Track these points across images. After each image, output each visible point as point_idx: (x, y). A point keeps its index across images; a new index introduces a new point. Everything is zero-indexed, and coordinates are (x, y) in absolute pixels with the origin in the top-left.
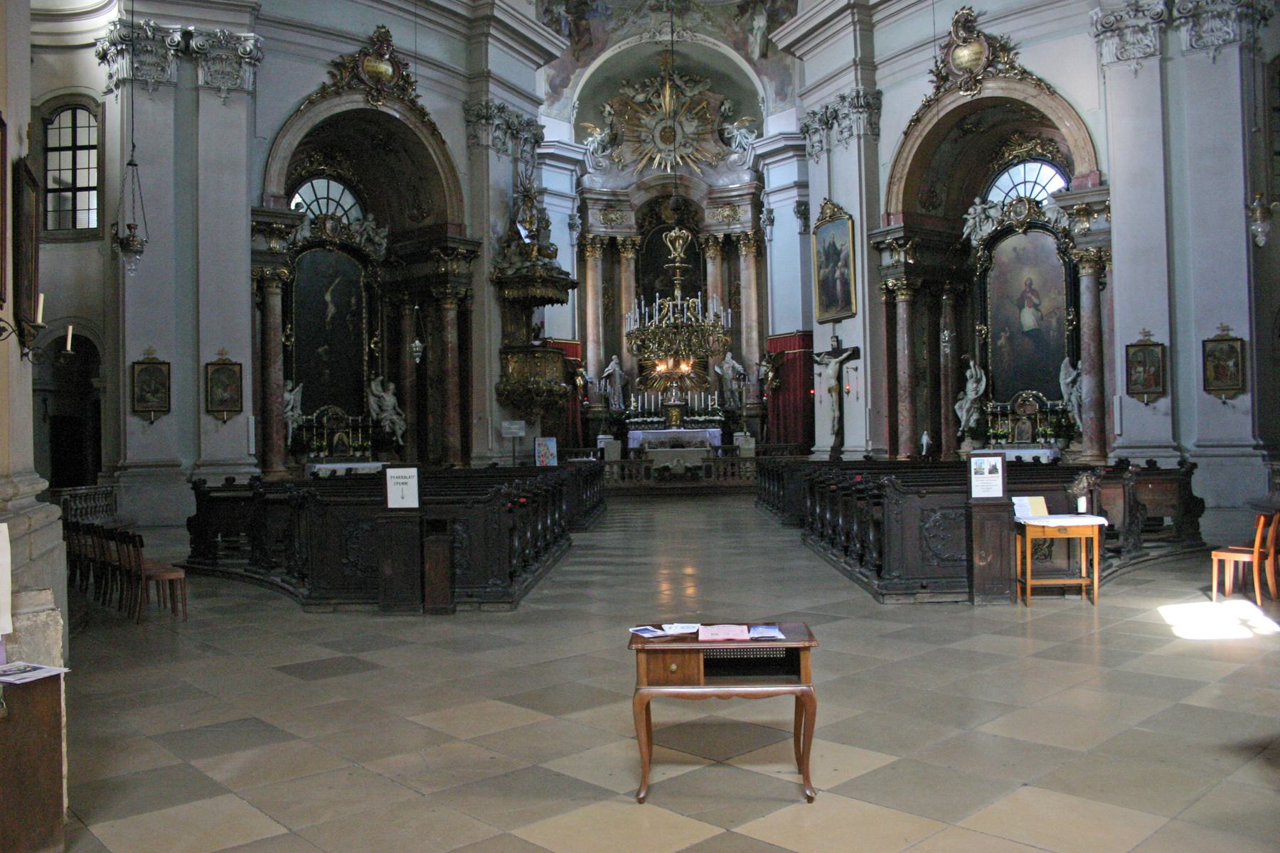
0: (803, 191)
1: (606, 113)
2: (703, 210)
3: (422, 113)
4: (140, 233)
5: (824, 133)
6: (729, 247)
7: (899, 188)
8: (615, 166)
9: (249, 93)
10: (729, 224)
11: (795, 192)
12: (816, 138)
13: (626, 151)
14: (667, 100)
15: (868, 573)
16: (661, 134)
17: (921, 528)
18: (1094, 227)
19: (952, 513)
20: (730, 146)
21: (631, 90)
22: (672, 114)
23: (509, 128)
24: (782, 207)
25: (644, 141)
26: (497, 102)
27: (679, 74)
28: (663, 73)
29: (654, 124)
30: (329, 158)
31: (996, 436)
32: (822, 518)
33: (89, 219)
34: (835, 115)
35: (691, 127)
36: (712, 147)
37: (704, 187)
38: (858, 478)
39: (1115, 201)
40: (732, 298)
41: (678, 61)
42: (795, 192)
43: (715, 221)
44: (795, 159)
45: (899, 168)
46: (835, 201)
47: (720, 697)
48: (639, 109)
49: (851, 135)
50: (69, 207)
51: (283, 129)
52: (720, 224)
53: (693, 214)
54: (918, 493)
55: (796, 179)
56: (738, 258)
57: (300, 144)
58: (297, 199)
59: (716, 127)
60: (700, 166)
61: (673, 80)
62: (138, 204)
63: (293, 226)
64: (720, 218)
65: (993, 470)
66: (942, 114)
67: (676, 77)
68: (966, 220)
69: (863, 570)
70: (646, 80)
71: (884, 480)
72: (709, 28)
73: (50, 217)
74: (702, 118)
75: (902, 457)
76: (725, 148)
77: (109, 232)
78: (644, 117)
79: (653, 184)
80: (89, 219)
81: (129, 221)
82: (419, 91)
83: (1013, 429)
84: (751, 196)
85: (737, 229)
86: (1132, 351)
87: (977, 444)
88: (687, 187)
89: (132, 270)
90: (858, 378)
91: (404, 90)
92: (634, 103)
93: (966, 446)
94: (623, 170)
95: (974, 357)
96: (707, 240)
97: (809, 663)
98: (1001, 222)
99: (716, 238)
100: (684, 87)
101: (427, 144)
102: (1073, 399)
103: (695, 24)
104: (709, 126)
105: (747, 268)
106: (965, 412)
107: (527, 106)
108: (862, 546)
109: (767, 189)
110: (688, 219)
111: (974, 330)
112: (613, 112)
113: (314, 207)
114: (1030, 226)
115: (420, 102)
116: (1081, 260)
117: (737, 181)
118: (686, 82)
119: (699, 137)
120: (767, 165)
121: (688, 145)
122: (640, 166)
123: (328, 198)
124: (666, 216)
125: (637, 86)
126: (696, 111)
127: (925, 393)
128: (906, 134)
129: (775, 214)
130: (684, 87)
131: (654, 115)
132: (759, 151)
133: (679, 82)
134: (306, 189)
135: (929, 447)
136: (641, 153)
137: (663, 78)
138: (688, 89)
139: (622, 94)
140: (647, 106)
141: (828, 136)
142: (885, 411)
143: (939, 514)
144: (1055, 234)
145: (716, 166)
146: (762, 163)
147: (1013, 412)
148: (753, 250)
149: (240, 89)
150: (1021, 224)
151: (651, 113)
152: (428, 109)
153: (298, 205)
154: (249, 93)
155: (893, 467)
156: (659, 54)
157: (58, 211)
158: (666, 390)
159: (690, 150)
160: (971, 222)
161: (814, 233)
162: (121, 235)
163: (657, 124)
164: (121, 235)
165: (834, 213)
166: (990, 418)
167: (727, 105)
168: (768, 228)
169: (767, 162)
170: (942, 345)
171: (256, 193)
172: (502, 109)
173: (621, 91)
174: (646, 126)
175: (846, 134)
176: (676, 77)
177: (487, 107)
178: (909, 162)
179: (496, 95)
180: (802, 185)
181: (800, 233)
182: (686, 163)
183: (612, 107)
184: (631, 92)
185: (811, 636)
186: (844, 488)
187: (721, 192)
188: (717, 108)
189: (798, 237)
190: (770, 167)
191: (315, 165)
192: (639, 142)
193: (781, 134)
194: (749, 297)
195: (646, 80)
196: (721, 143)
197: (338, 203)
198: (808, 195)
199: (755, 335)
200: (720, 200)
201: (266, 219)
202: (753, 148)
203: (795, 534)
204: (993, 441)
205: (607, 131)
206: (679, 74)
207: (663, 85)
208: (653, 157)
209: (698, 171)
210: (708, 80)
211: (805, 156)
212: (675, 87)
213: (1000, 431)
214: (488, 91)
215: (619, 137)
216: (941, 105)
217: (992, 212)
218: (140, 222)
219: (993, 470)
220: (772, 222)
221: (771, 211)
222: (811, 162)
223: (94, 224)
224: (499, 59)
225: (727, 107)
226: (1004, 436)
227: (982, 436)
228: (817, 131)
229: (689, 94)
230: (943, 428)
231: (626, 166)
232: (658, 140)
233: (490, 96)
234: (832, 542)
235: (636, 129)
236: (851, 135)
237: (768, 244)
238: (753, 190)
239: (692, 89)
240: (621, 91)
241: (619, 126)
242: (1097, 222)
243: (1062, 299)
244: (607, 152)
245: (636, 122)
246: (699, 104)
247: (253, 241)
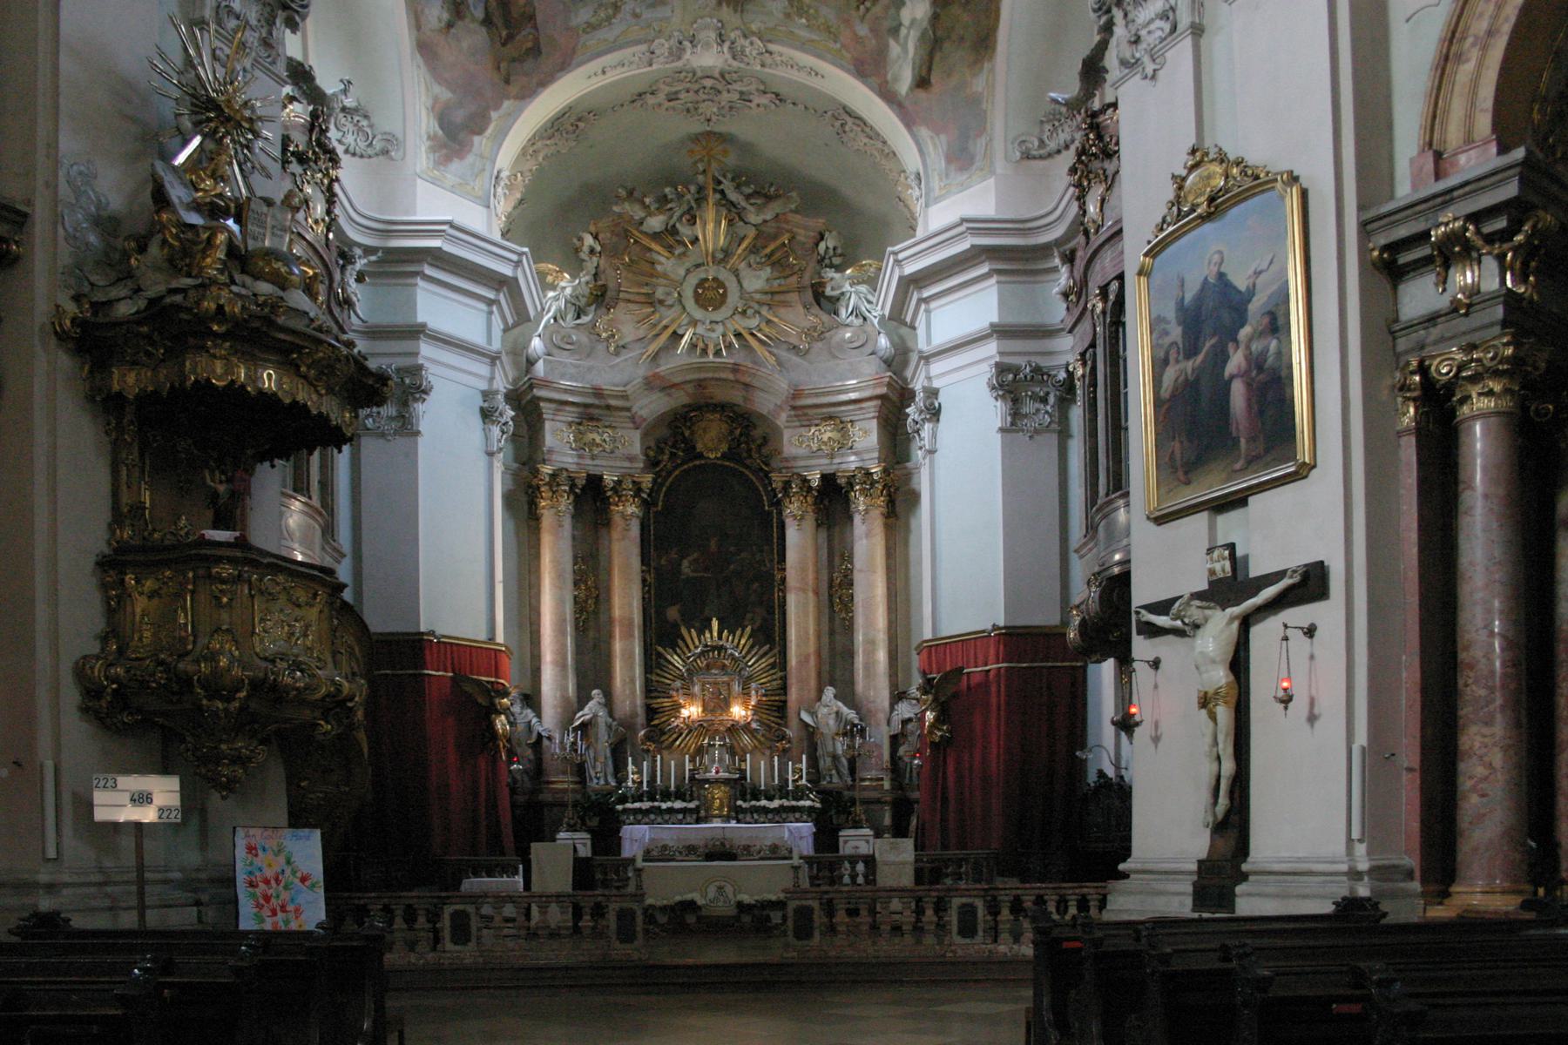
1: (583, 255)
8: (601, 347)
13: (626, 322)
14: (711, 231)
16: (696, 292)
20: (836, 313)
21: (637, 207)
22: (720, 256)
25: (661, 302)
27: (733, 180)
28: (701, 178)
29: (682, 272)
35: (757, 280)
36: (796, 319)
41: (731, 160)
44: (993, 280)
48: (654, 246)
52: (814, 454)
53: (759, 442)
55: (995, 319)
59: (807, 279)
60: (775, 351)
61: (722, 192)
67: (727, 186)
70: (667, 190)
72: (804, 34)
74: (778, 263)
76: (825, 317)
78: (662, 259)
79: (677, 380)
84: (878, 402)
85: (852, 462)
88: (747, 385)
92: (646, 234)
94: (617, 354)
100: (743, 203)
103: (771, 25)
104: (794, 279)
110: (749, 451)
112: (598, 248)
118: (748, 197)
119: (774, 298)
120: (926, 300)
121: (750, 312)
122: (653, 347)
124: (705, 445)
125: (647, 200)
126: (768, 251)
130: (743, 203)
131: (684, 254)
132: (910, 269)
133: (733, 196)
136: (655, 325)
137: (701, 189)
138: (751, 208)
139: (620, 215)
140: (668, 236)
145: (807, 352)
151: (677, 252)
156: (696, 138)
158: (700, 751)
159: (753, 322)
163: (688, 271)
167: (830, 242)
169: (926, 294)
173: (616, 209)
174: (665, 276)
176: (727, 186)
182: (746, 346)
183: (596, 237)
184: (638, 213)
187: (817, 395)
188: (810, 245)
190: (933, 305)
192: (651, 304)
193: (964, 220)
195: (667, 190)
196: (816, 309)
202: (898, 262)
205: (585, 278)
206: (733, 180)
207: (701, 199)
208: (680, 332)
210: (794, 194)
212: (725, 202)
215: (609, 294)
225: (831, 245)
229: (754, 218)
231: (623, 347)
232: (690, 303)
235: (647, 279)
238: (884, 390)
239: (760, 209)
240: (616, 209)
241: (610, 272)
244: (585, 319)
245: (646, 267)
246: (775, 237)
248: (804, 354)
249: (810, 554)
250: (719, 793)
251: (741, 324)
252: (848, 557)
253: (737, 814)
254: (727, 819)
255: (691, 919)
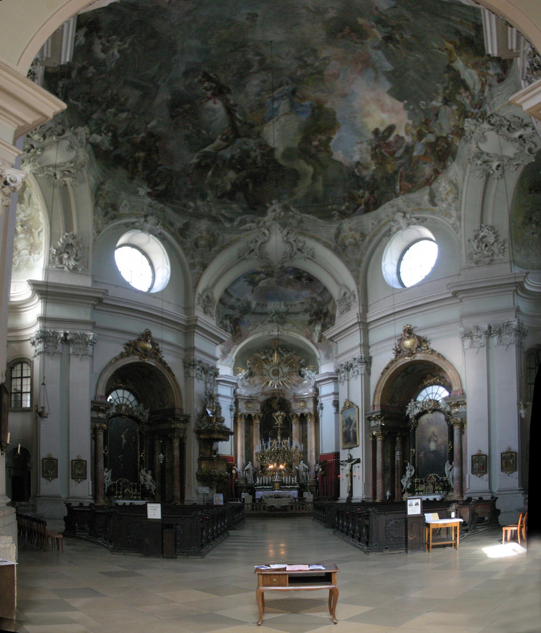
0: (336, 396)
2: (291, 404)
3: (164, 364)
4: (46, 410)
5: (346, 373)
6: (303, 419)
7: (379, 395)
9: (90, 356)
10: (303, 409)
11: (333, 396)
12: (343, 375)
15: (362, 544)
17: (385, 527)
18: (460, 411)
19: (399, 521)
23: (203, 369)
24: (327, 403)
26: (198, 359)
30: (124, 381)
31: (418, 491)
32: (342, 525)
33: (27, 404)
34: (351, 366)
37: (292, 394)
38: (359, 509)
39: (469, 401)
40: (304, 439)
42: (333, 396)
43: (297, 408)
45: (379, 387)
46: (351, 400)
47: (295, 590)
49: (358, 374)
50: (20, 399)
51: (105, 369)
52: (298, 409)
54: (385, 514)
56: (306, 423)
57: (112, 376)
58: (110, 397)
62: (46, 399)
63: (108, 408)
64: (299, 407)
65: (417, 504)
66: (398, 366)
68: (407, 408)
69: (360, 543)
71: (370, 510)
73: (13, 402)
75: (378, 500)
77: (34, 409)
79: (268, 393)
80: (27, 404)
81: (42, 405)
82: (163, 355)
83: (425, 488)
85: (306, 411)
86: (474, 457)
87: (410, 494)
89: (44, 424)
90: (359, 471)
91: (156, 354)
93: (406, 496)
95: (409, 461)
96: (293, 416)
97: (336, 578)
98: (422, 409)
99: (297, 415)
101: (166, 376)
102: (450, 476)
105: (311, 427)
106: (405, 482)
107: (212, 361)
108: (360, 535)
109: (320, 395)
111: (410, 451)
113: (117, 400)
114: (434, 410)
115: (164, 359)
116: (454, 423)
117: (307, 392)
123: (123, 397)
127: (388, 476)
128: (382, 374)
129: (324, 405)
134: (114, 393)
135: (390, 496)
141: (348, 374)
142: (371, 483)
143: (393, 522)
144: (444, 414)
146: (318, 385)
147: (426, 482)
148: (314, 420)
149: (87, 355)
150: (430, 410)
152: (167, 362)
153: (110, 400)
154: (90, 356)
155: (374, 504)
157: (16, 401)
160: (409, 409)
161: (341, 413)
162: (39, 411)
164: (39, 411)
165: (350, 405)
166: (416, 485)
168: (320, 411)
170: (396, 457)
171: (93, 394)
172: (200, 362)
175: (356, 373)
177: (194, 361)
178: (383, 385)
179: (198, 356)
180: (336, 394)
181: (335, 413)
182: (283, 384)
185: (337, 568)
186: (352, 513)
189: (334, 415)
191: (118, 384)
194: (311, 439)
197: (128, 399)
198: (338, 398)
199: (314, 454)
200: (299, 399)
201: (97, 405)
203: (331, 531)
204: (417, 493)
209: (289, 387)
211: (337, 382)
213: (420, 489)
214: (194, 355)
216: (398, 362)
217: (418, 405)
218: (46, 406)
219: (417, 504)
220: (322, 408)
221: (322, 404)
222: (340, 385)
223: (29, 406)
224: (199, 342)
226: (422, 491)
227: (412, 491)
228: (343, 372)
230: (396, 489)
233: (195, 357)
234: (347, 534)
236: (358, 374)
237: (320, 417)
238: (314, 396)
242: (461, 409)
243: (447, 438)
247: (92, 414)
248: (296, 386)
249: (298, 431)
250: (277, 485)
251: (283, 379)
252: (306, 431)
253: (281, 489)
254: (279, 490)
255: (273, 508)
